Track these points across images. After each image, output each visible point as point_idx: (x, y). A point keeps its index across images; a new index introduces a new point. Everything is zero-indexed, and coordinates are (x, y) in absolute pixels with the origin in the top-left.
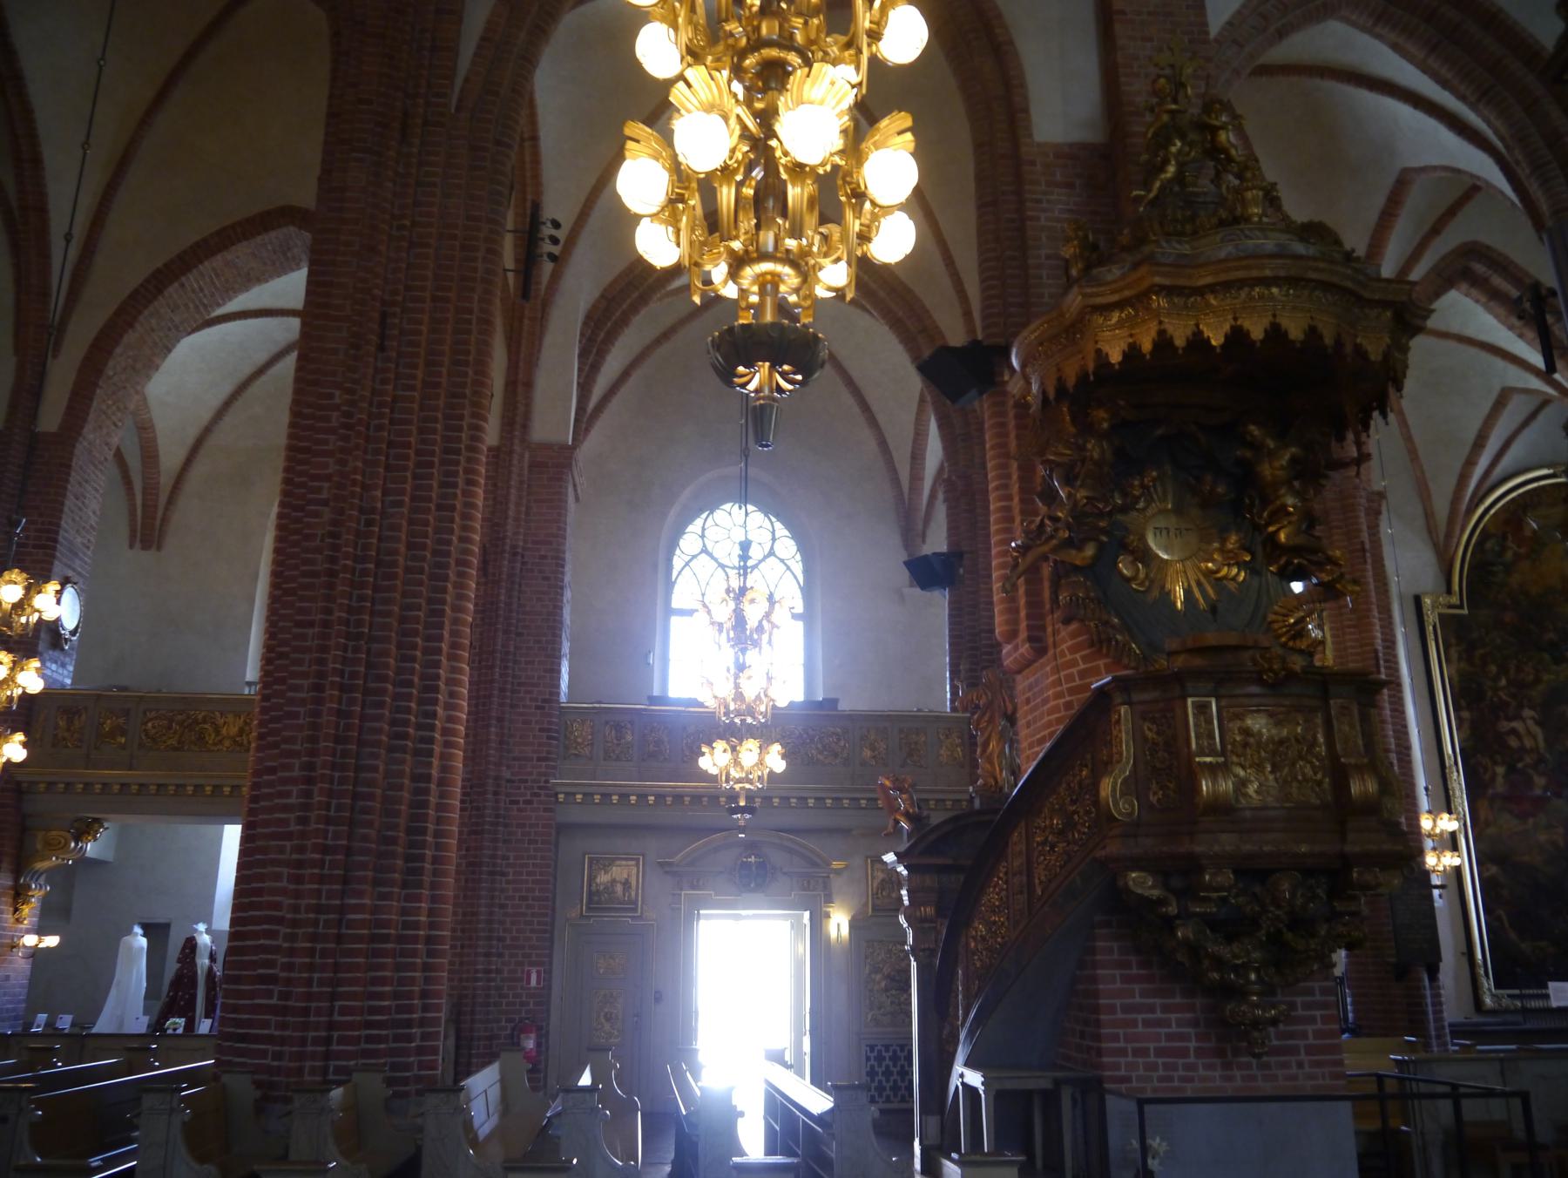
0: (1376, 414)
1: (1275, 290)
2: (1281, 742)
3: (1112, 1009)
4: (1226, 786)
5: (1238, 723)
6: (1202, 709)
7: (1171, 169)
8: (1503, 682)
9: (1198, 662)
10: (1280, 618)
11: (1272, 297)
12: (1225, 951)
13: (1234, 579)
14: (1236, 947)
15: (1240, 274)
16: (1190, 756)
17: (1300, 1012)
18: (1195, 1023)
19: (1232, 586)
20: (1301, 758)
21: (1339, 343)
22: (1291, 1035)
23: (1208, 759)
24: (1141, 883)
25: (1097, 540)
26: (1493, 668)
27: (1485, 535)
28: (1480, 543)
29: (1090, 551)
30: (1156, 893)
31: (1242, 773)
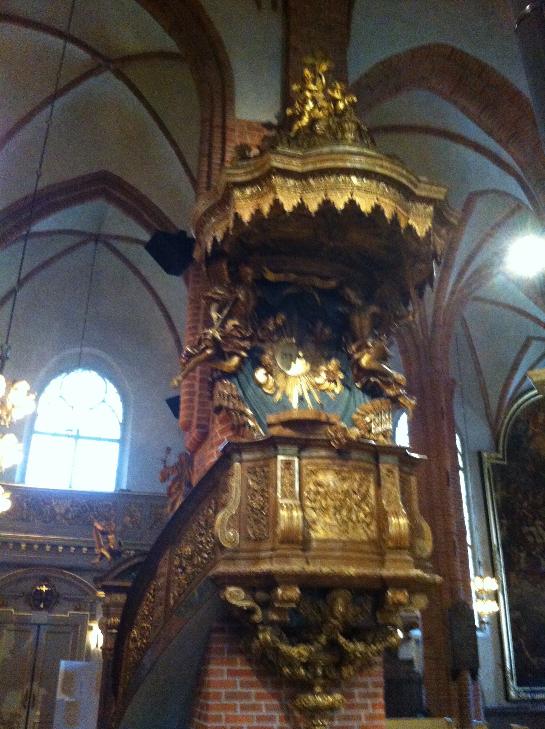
3: (218, 696)
6: (288, 465)
8: (526, 504)
9: (288, 432)
10: (360, 417)
17: (358, 700)
19: (331, 395)
21: (395, 217)
25: (239, 355)
26: (520, 496)
27: (517, 421)
28: (515, 425)
30: (246, 604)
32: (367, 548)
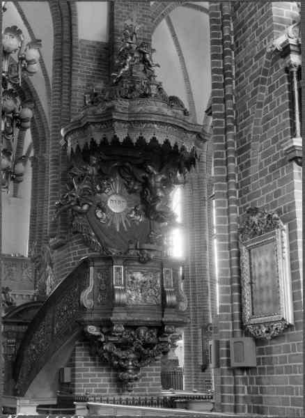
0: (193, 166)
1: (156, 126)
2: (144, 282)
4: (123, 297)
5: (130, 275)
7: (127, 67)
11: (154, 128)
12: (121, 354)
13: (138, 221)
14: (124, 353)
15: (143, 119)
16: (113, 286)
18: (110, 381)
19: (138, 223)
20: (151, 288)
21: (176, 146)
22: (144, 385)
23: (118, 287)
24: (93, 330)
29: (85, 207)
30: (97, 333)
31: (130, 292)
32: (155, 307)
